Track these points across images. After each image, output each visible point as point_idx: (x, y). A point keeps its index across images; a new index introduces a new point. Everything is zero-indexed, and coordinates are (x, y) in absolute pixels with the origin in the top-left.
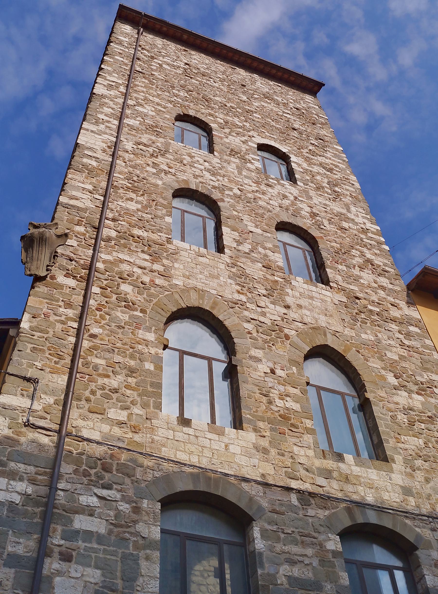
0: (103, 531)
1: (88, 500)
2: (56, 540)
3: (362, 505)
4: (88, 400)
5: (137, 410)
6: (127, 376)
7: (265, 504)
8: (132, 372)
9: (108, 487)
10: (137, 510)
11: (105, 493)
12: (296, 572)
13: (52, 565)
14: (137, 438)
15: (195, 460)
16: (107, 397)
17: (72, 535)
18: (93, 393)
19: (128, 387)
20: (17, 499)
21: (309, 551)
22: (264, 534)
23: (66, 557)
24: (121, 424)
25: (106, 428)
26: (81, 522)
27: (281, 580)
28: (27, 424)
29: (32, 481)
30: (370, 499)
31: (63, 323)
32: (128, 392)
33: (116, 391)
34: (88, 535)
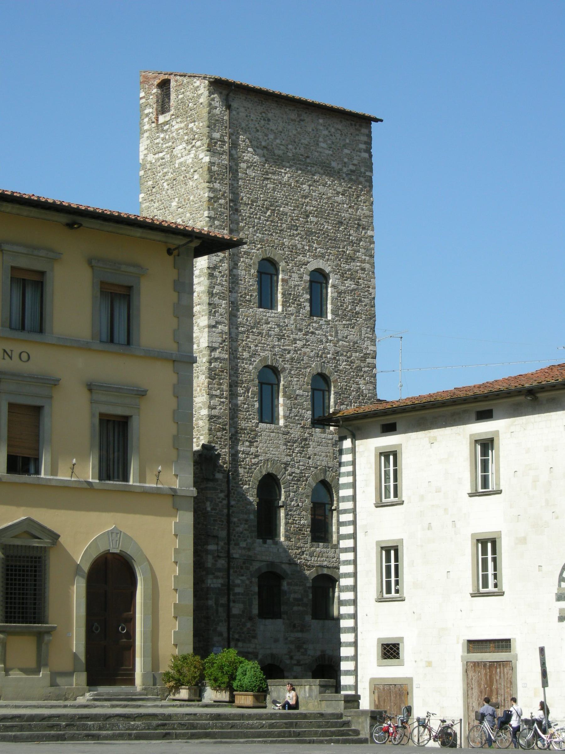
0: (243, 592)
1: (238, 582)
2: (231, 597)
3: (322, 567)
4: (234, 540)
5: (249, 540)
6: (245, 524)
7: (289, 572)
8: (247, 521)
9: (242, 575)
10: (251, 582)
11: (241, 578)
12: (296, 596)
13: (232, 604)
14: (250, 553)
15: (268, 558)
16: (239, 536)
17: (235, 594)
18: (235, 536)
19: (245, 530)
20: (220, 586)
21: (301, 588)
22: (288, 584)
23: (234, 602)
24: (244, 548)
25: (240, 551)
26: (237, 590)
27: (291, 600)
28: (219, 557)
29: (222, 578)
30: (325, 563)
31: (221, 502)
32: (245, 532)
33: (242, 533)
34: (239, 594)
